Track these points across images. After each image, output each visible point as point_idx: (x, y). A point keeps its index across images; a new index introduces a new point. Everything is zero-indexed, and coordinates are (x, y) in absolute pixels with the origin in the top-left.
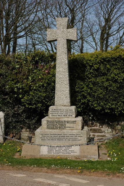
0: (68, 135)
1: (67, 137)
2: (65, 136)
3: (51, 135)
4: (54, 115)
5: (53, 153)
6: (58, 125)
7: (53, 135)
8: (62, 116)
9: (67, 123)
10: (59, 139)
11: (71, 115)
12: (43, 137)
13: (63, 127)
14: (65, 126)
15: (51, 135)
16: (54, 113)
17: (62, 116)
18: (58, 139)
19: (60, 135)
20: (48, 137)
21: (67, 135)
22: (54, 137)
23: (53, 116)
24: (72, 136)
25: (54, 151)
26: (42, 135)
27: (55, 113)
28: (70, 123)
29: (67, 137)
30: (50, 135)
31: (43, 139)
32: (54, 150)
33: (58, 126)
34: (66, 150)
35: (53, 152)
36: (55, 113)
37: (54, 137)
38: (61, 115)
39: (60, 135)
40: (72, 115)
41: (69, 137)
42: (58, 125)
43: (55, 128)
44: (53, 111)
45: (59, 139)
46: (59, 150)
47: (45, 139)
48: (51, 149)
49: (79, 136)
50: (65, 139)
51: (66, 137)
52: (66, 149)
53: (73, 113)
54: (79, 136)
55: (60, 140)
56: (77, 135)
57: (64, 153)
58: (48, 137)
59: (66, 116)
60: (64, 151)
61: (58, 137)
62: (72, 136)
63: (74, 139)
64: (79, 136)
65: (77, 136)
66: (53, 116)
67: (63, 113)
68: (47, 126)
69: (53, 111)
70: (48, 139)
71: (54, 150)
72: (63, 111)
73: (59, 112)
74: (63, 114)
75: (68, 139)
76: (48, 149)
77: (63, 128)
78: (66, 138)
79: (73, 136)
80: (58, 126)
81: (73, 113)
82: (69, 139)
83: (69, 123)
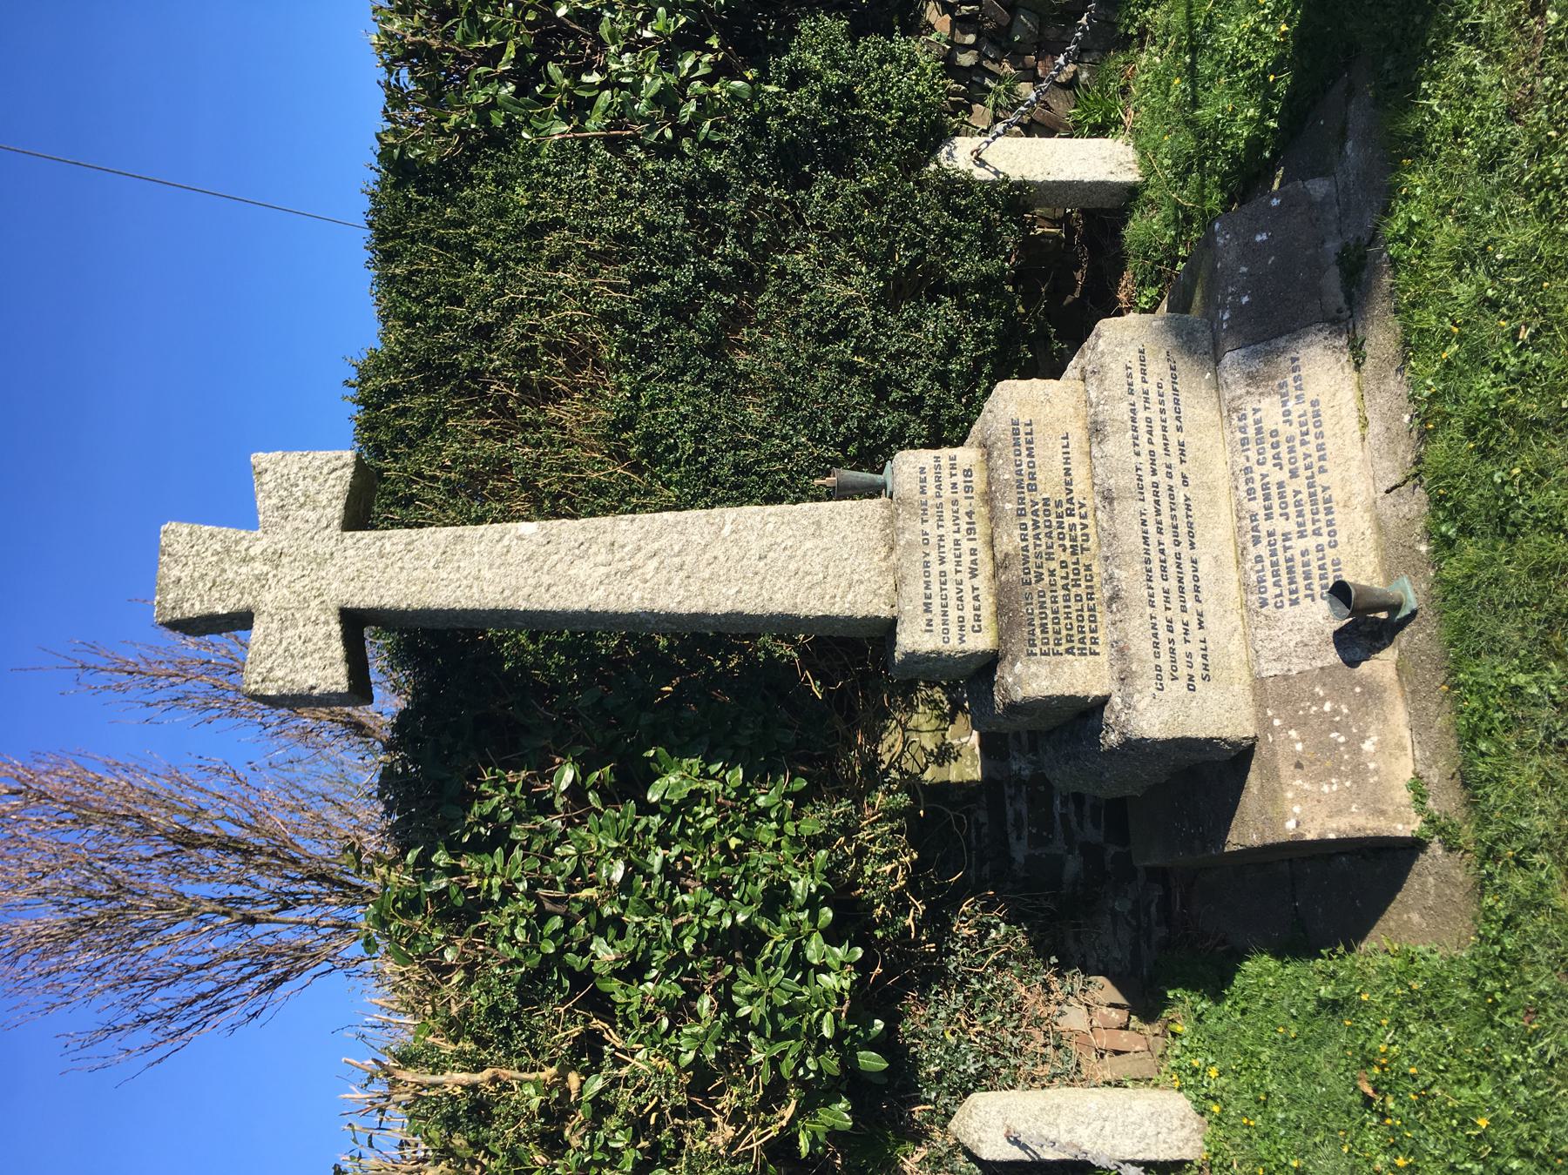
0: (1145, 457)
1: (1162, 471)
2: (1155, 485)
3: (1159, 599)
4: (969, 613)
5: (1334, 545)
6: (1054, 565)
7: (1158, 584)
8: (972, 545)
9: (1033, 488)
10: (1183, 529)
11: (960, 479)
12: (1183, 671)
13: (1067, 520)
14: (1059, 504)
15: (1159, 599)
16: (953, 614)
17: (972, 545)
18: (1185, 544)
19: (1152, 529)
20: (1178, 628)
21: (1146, 467)
22: (1172, 570)
23: (977, 618)
24: (1142, 425)
25: (1310, 542)
26: (1167, 681)
27: (953, 602)
28: (1032, 465)
29: (1162, 471)
30: (1159, 612)
31: (1198, 671)
32: (1298, 545)
33: (1064, 565)
34: (1283, 448)
35: (1320, 548)
36: (953, 602)
37: (1172, 570)
38: (966, 559)
39: (1152, 529)
40: (959, 472)
41: (1159, 450)
42: (1054, 565)
43: (1082, 591)
44: (937, 621)
45: (1183, 529)
46: (1291, 510)
47: (1195, 648)
48: (1292, 581)
49: (1144, 372)
50: (1177, 481)
51: (1161, 477)
52: (1270, 453)
53: (945, 462)
54: (1137, 376)
55: (1190, 525)
56: (1131, 392)
57: (1322, 458)
58: (1178, 628)
59: (970, 514)
60: (1301, 464)
61: (1167, 539)
62: (1142, 425)
63: (1170, 414)
64: (1144, 372)
65: (1138, 385)
66: (977, 618)
67: (949, 544)
68: (1069, 651)
69: (937, 621)
70: (1194, 625)
71: (1298, 545)
72: (933, 541)
73: (943, 574)
74: (957, 542)
75: (1175, 461)
76: (1294, 602)
77: (1076, 520)
78: (1169, 475)
79: (1155, 485)
80: (1064, 565)
81: (945, 462)
82: (1174, 449)
83: (1032, 476)
